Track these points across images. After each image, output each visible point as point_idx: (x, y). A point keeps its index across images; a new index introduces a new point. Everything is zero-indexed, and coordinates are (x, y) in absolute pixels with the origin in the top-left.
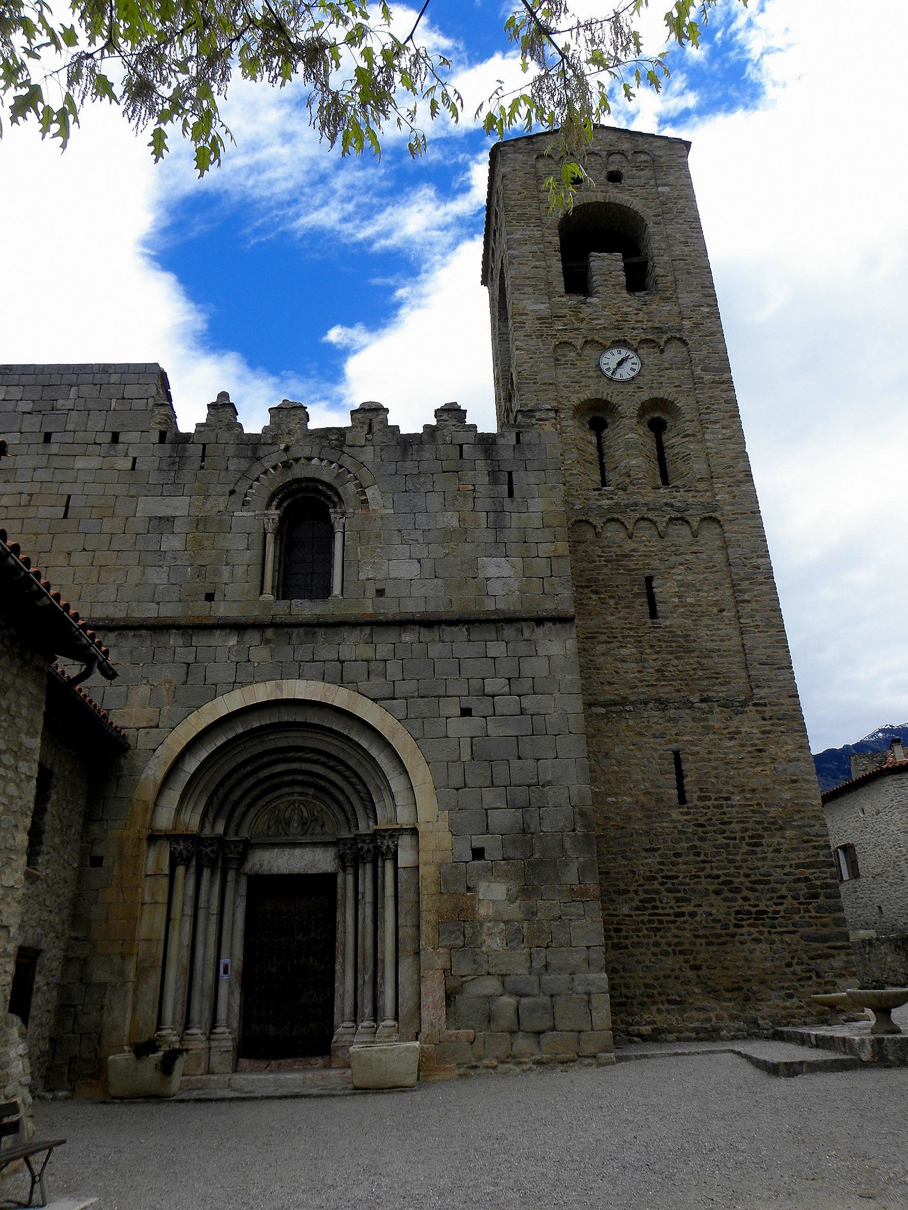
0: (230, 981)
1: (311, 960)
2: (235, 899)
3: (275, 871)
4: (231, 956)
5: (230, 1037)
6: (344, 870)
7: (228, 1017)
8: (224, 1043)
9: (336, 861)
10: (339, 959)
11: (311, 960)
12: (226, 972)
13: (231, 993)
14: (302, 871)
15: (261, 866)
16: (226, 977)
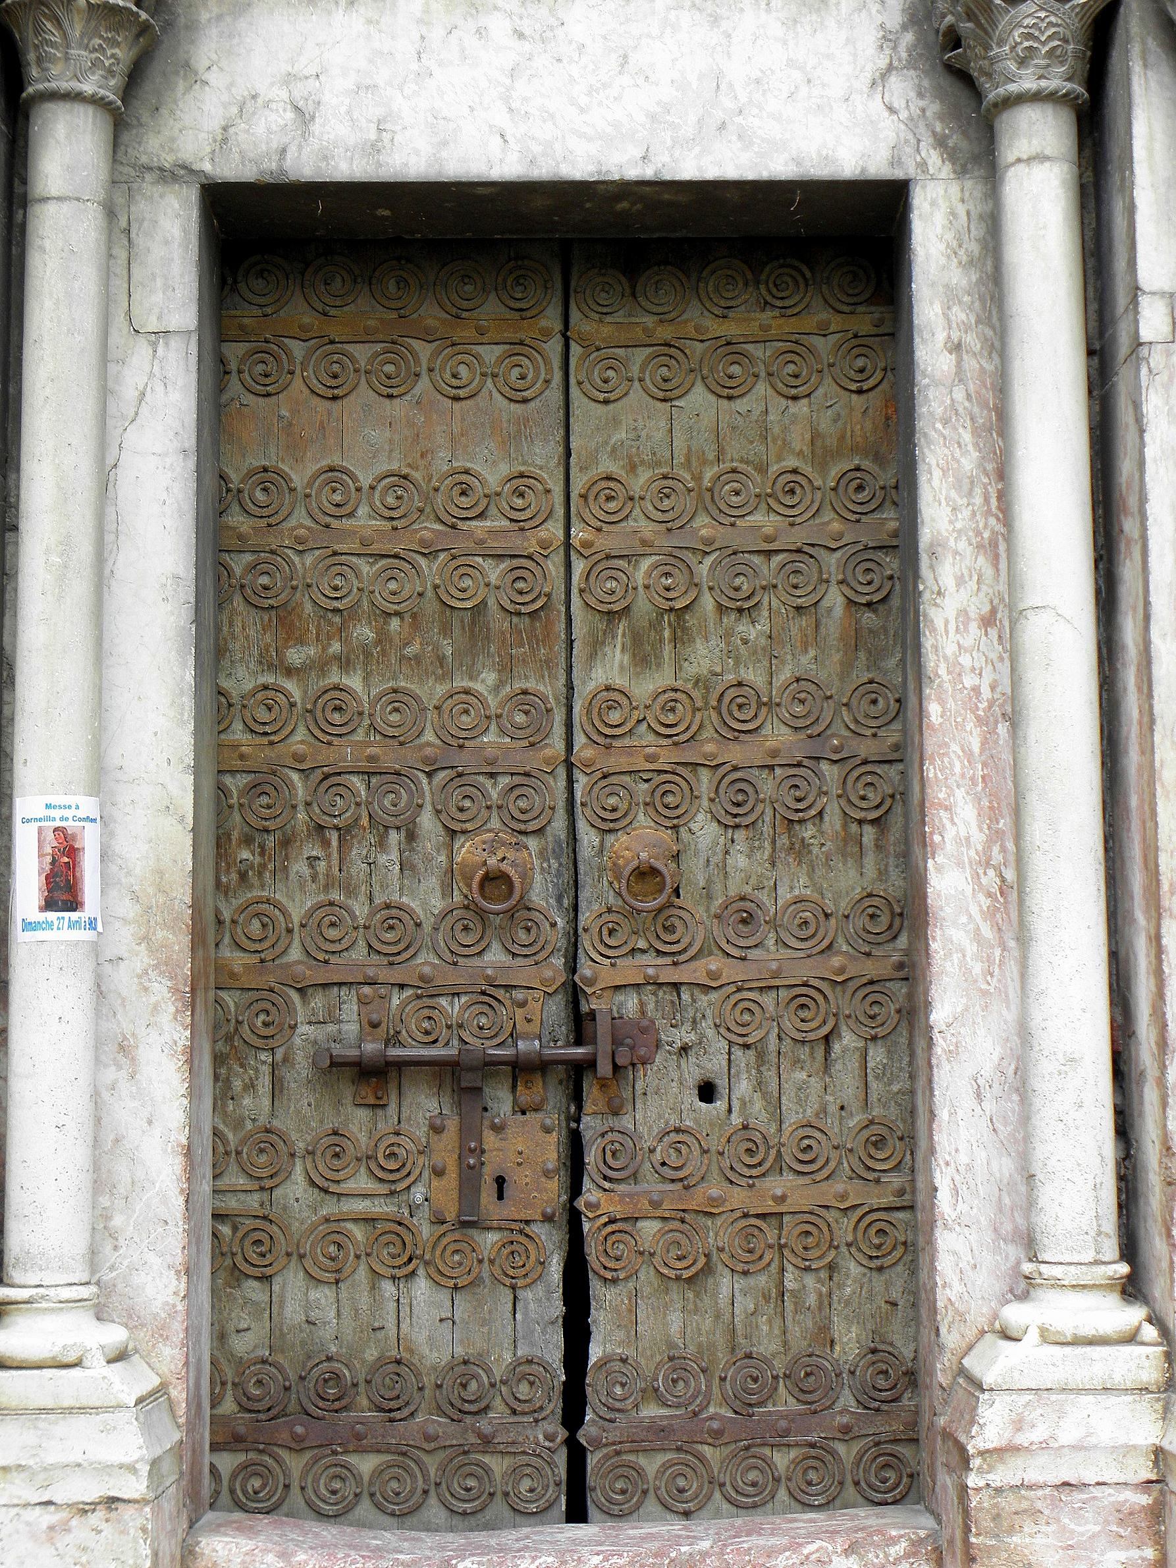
0: (100, 962)
1: (704, 831)
2: (106, 359)
3: (413, 157)
4: (100, 776)
5: (128, 1383)
6: (977, 138)
7: (101, 1233)
8: (73, 1441)
9: (902, 89)
10: (956, 825)
11: (704, 831)
12: (62, 891)
13: (113, 1049)
14: (625, 162)
15: (304, 116)
16: (63, 930)
